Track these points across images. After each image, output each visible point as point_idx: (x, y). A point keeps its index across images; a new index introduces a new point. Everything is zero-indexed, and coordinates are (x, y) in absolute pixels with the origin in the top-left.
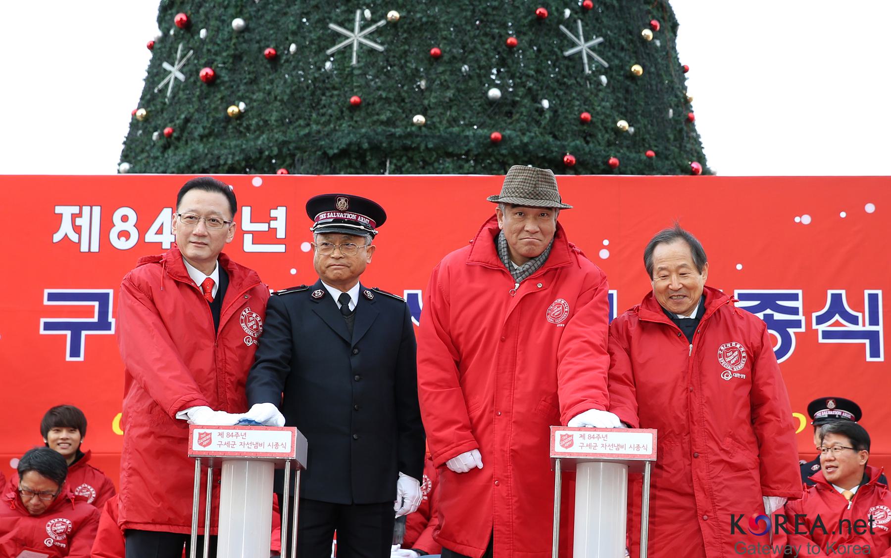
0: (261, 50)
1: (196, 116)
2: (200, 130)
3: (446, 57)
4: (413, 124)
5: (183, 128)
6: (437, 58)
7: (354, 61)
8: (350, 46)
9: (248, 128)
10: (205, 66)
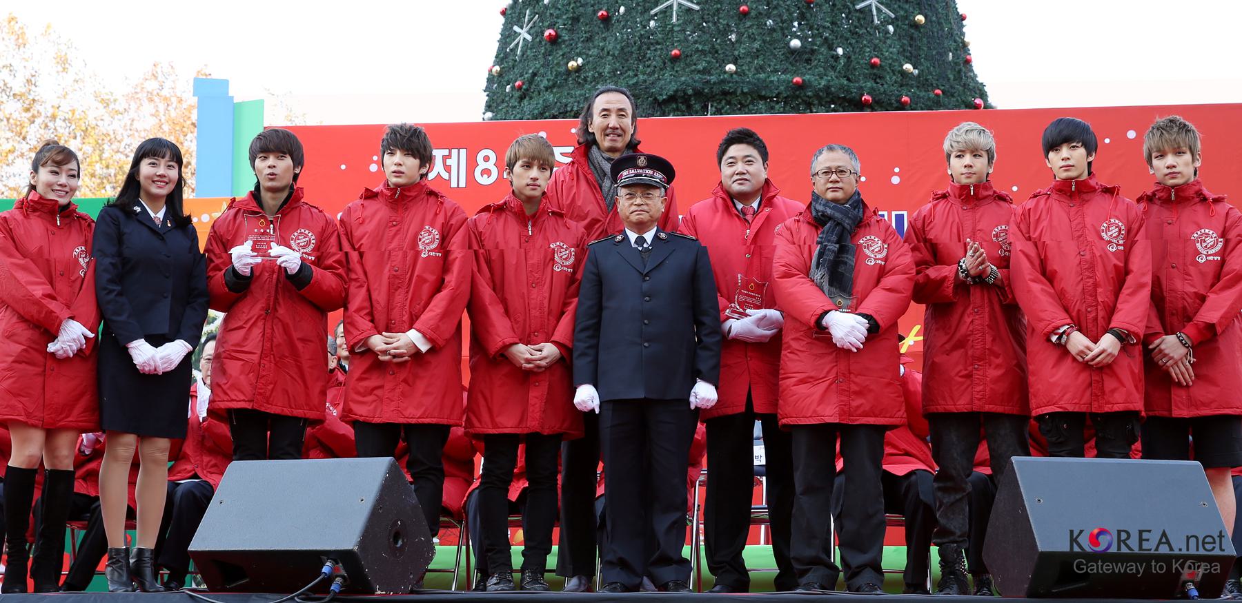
0: (595, 12)
1: (542, 70)
2: (545, 82)
3: (753, 13)
4: (725, 72)
5: (531, 81)
6: (745, 14)
7: (674, 20)
8: (671, 6)
9: (585, 80)
10: (548, 28)
